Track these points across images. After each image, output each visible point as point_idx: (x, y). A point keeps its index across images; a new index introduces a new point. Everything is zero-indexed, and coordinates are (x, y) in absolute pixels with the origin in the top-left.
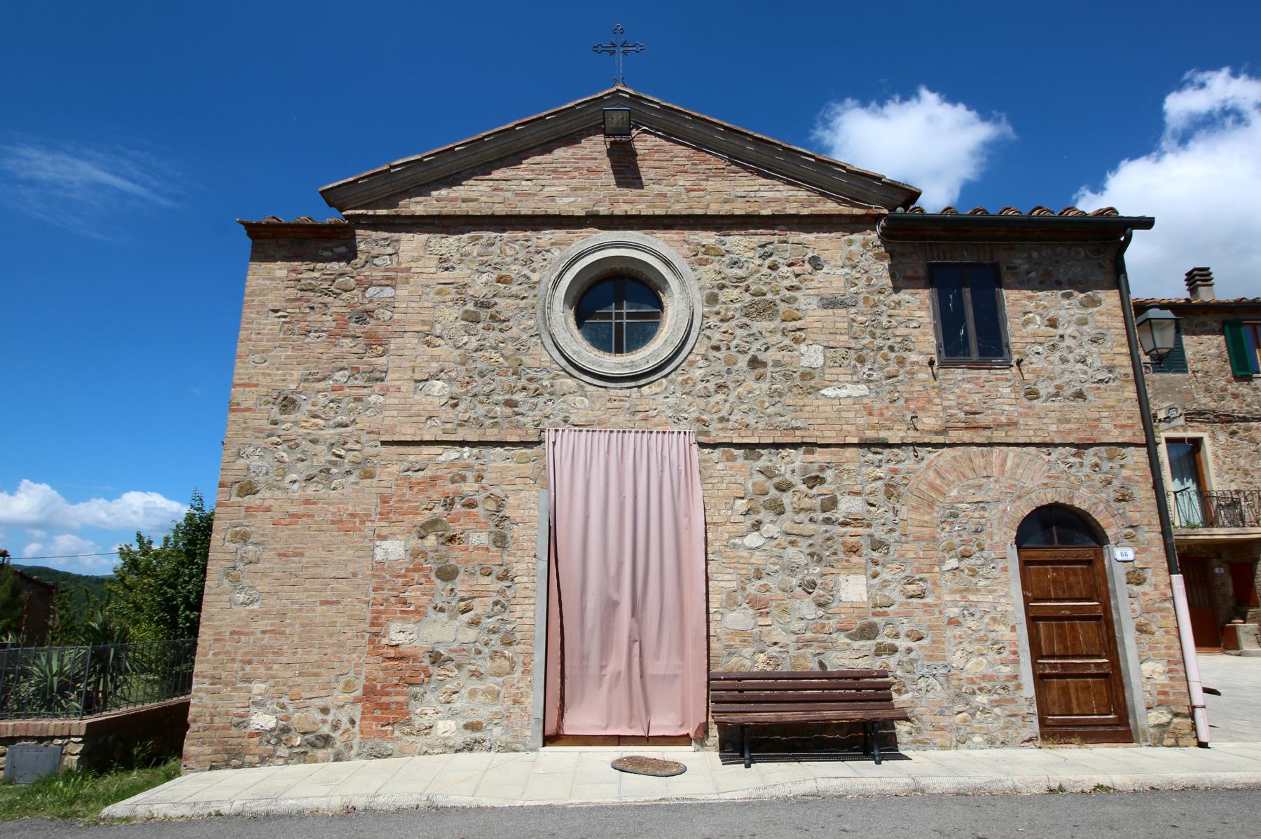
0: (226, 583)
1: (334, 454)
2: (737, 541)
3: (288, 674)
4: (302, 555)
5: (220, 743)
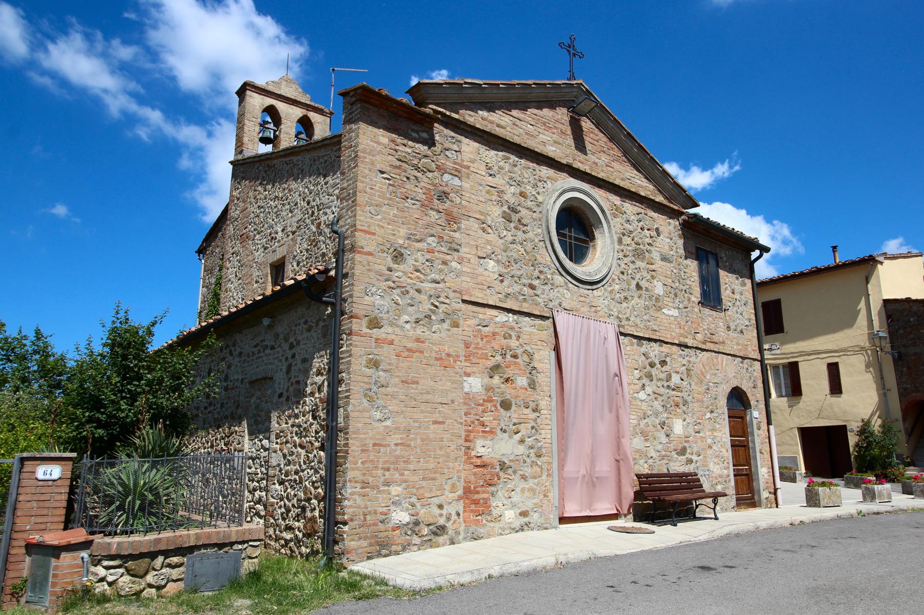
0: (366, 403)
1: (433, 304)
2: (636, 395)
3: (416, 478)
4: (417, 383)
5: (372, 537)
